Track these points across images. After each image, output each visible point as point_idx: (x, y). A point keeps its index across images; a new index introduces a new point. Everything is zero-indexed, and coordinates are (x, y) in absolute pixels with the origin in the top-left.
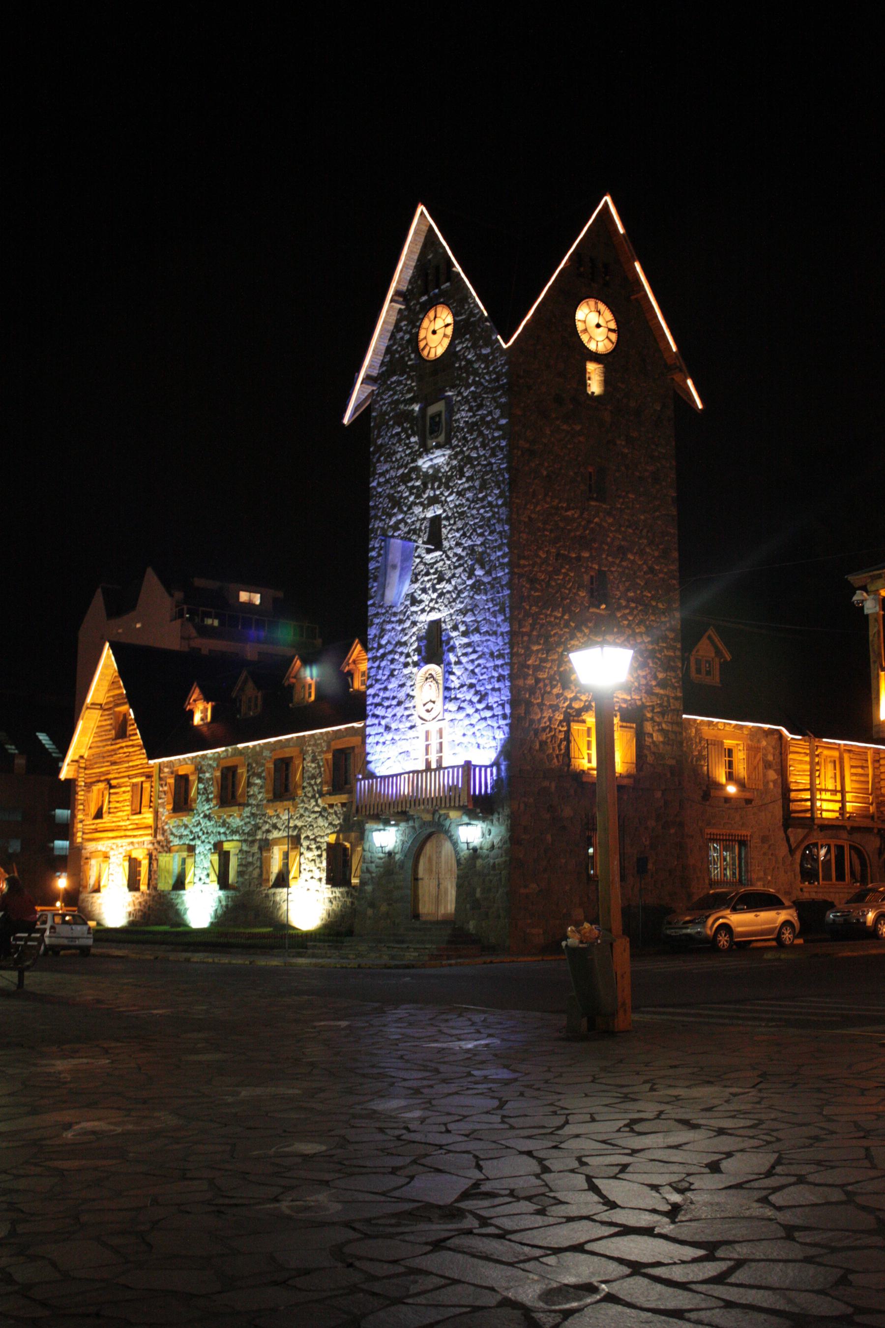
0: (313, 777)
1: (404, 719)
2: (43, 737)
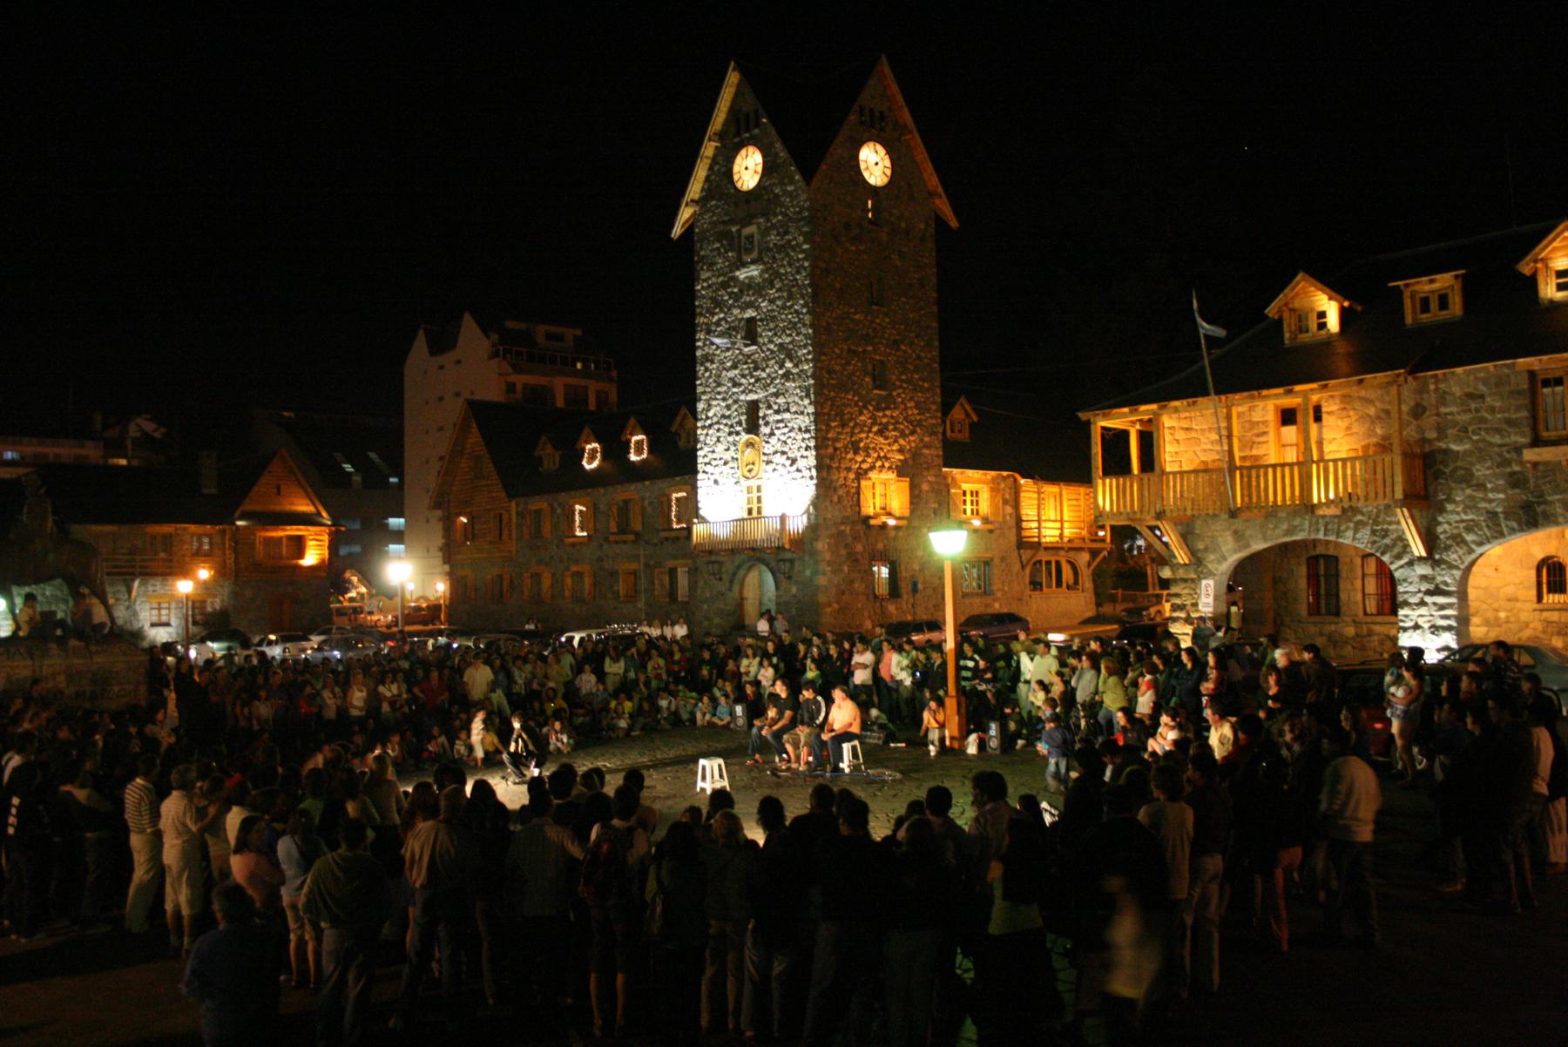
2: (373, 455)
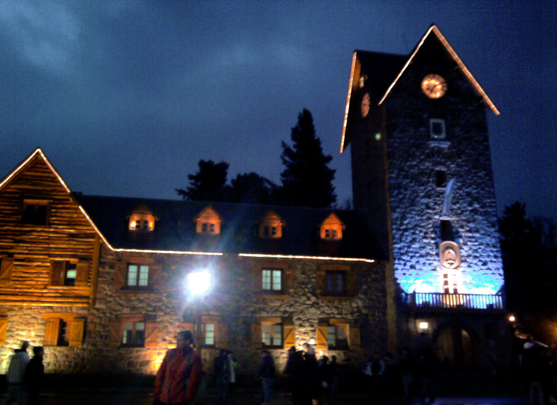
0: (303, 283)
1: (427, 265)
